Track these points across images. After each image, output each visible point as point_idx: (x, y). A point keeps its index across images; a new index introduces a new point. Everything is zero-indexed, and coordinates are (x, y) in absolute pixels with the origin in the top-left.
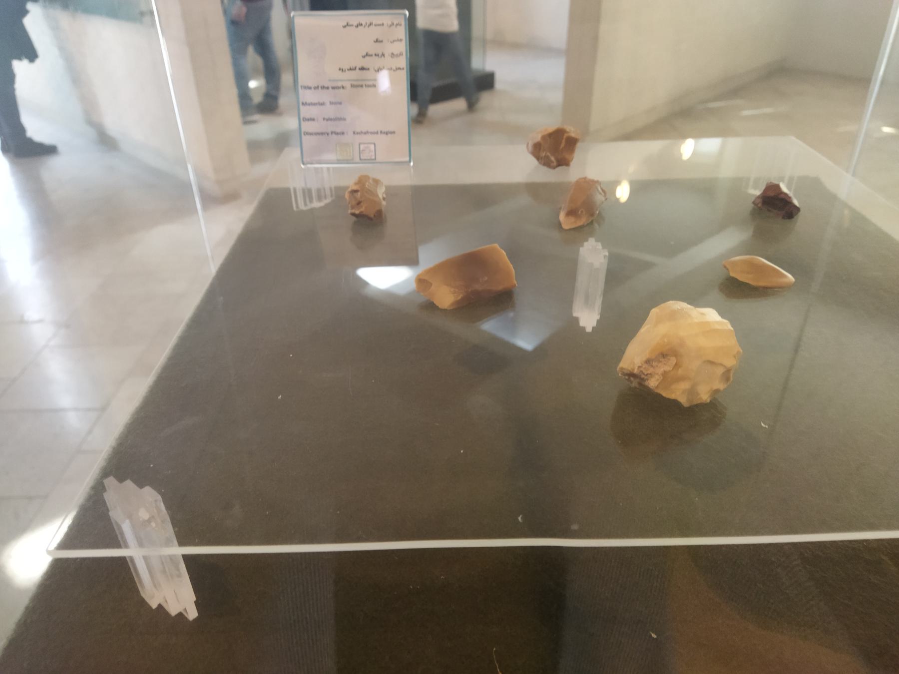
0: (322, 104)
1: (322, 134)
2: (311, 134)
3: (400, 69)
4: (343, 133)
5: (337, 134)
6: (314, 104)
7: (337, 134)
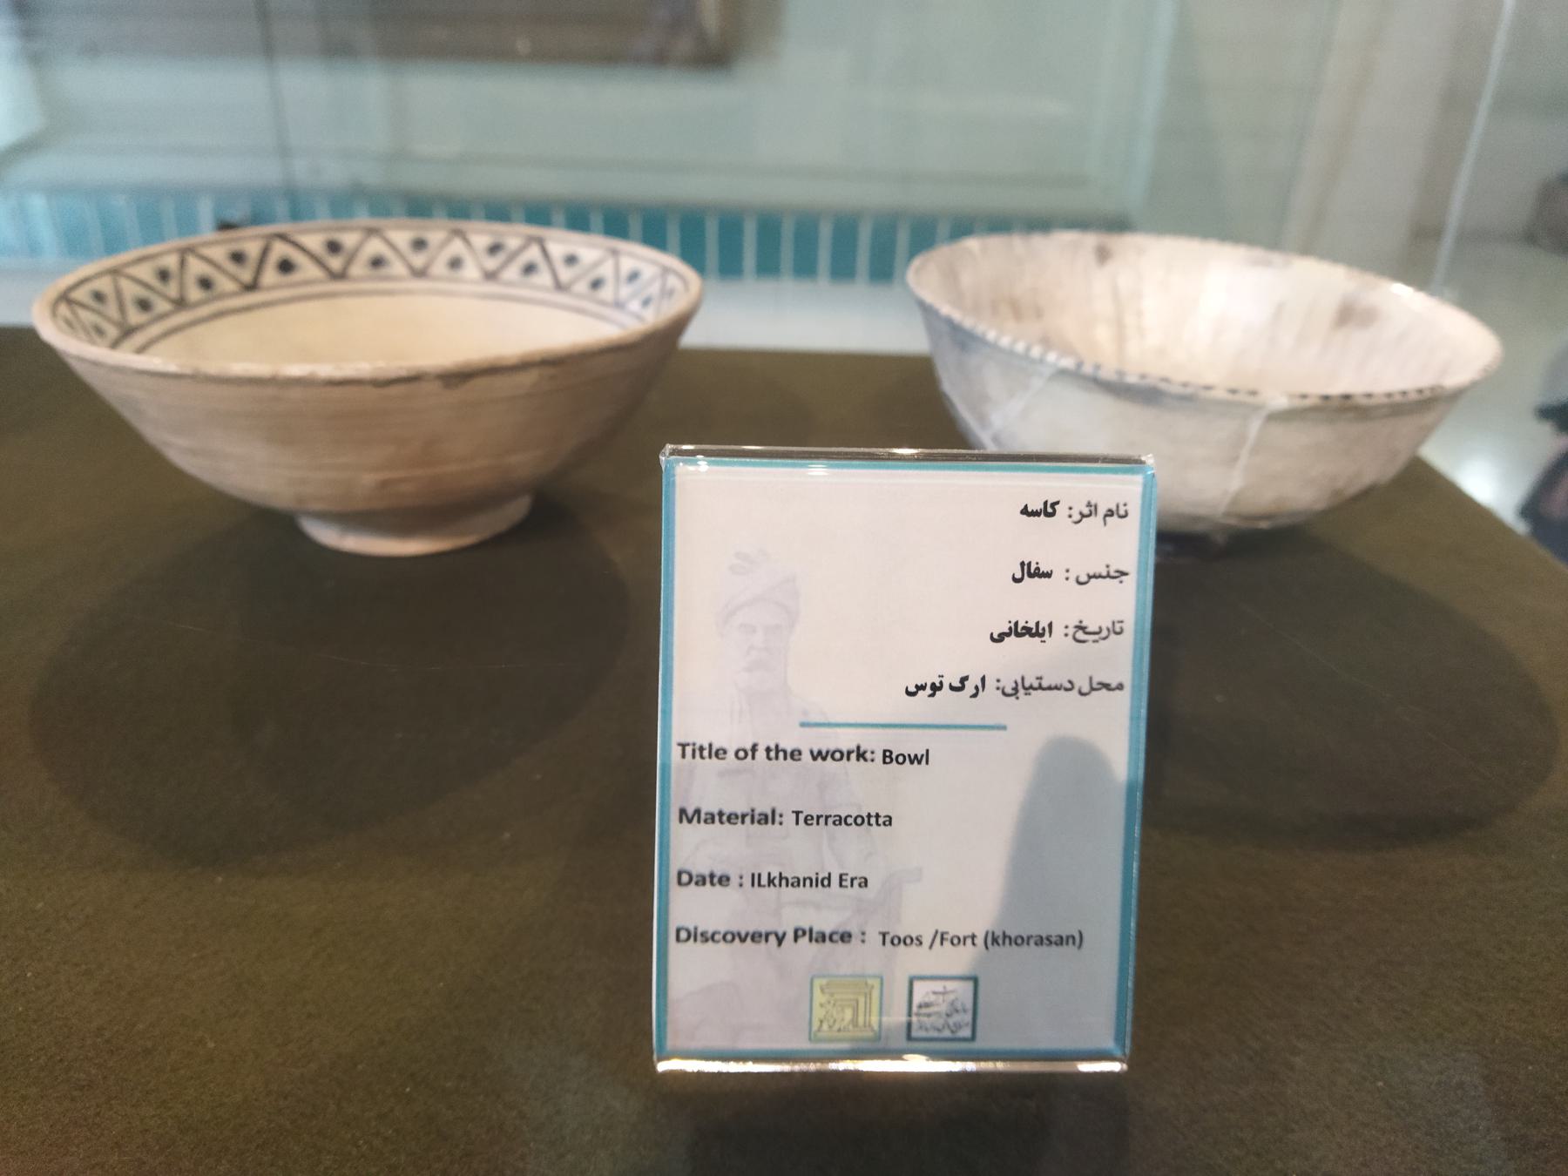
0: (765, 819)
1: (756, 937)
2: (708, 938)
3: (1107, 686)
4: (845, 937)
5: (822, 938)
6: (732, 818)
7: (822, 938)
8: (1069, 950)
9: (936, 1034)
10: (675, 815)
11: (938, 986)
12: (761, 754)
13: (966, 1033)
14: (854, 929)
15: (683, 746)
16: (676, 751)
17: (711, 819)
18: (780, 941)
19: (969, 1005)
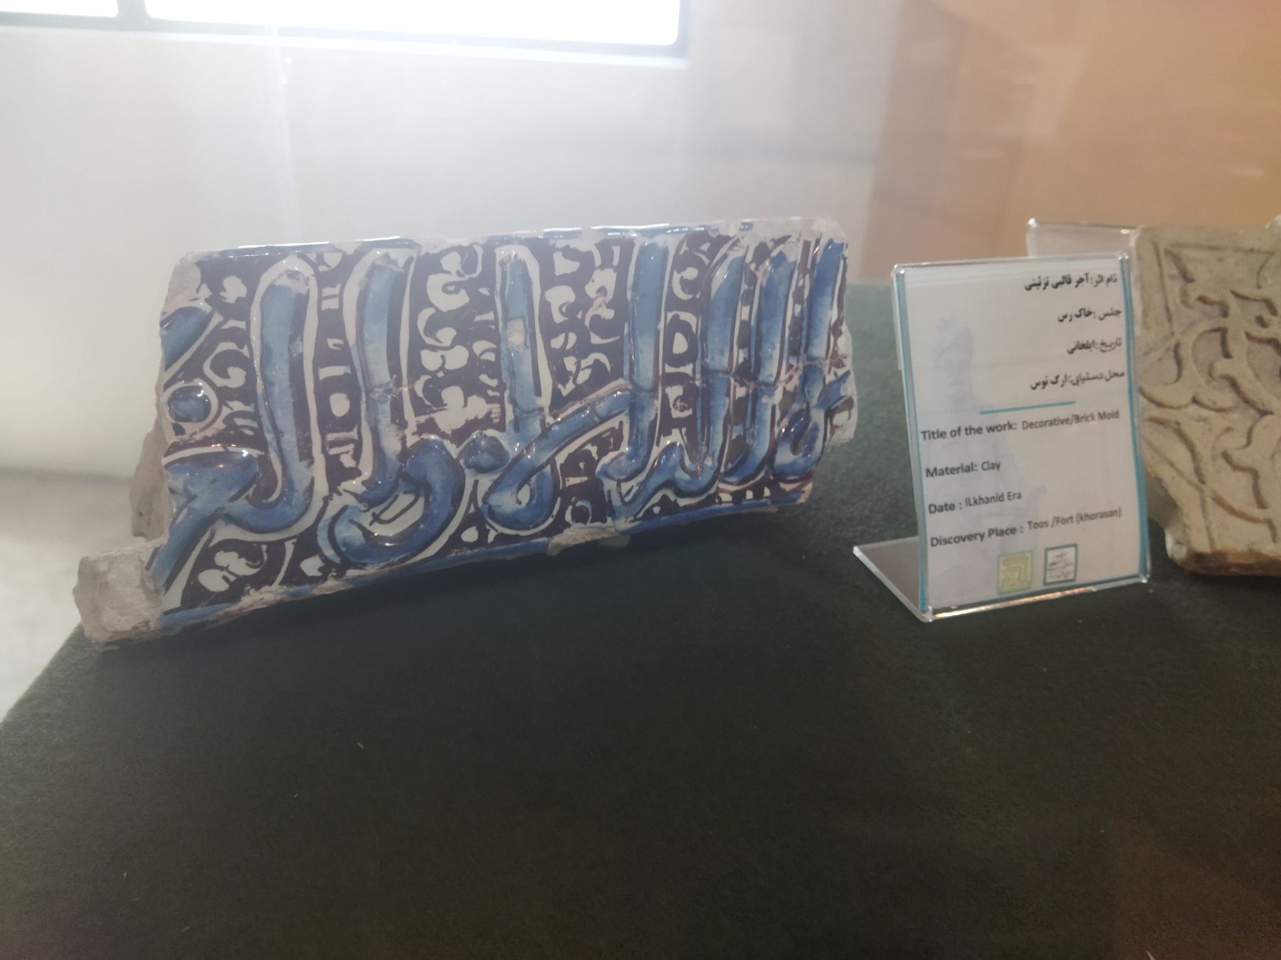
0: (969, 469)
1: (970, 537)
2: (947, 541)
3: (1116, 375)
4: (1013, 531)
5: (1002, 533)
6: (953, 471)
7: (1002, 533)
8: (1115, 518)
9: (1057, 579)
10: (924, 474)
11: (1057, 552)
12: (963, 432)
13: (1071, 576)
14: (1017, 525)
15: (924, 433)
16: (921, 436)
17: (942, 472)
18: (982, 537)
19: (1073, 560)
